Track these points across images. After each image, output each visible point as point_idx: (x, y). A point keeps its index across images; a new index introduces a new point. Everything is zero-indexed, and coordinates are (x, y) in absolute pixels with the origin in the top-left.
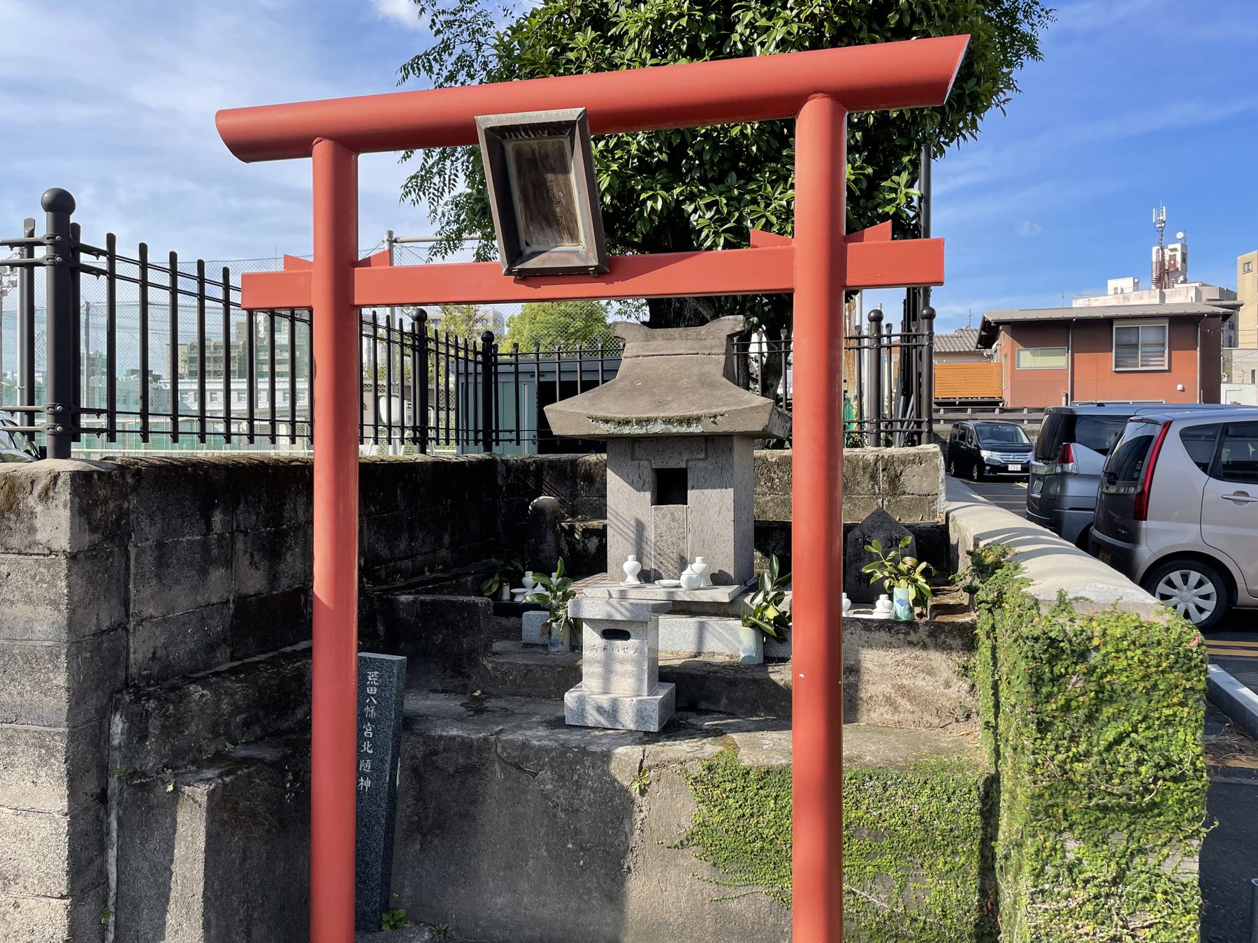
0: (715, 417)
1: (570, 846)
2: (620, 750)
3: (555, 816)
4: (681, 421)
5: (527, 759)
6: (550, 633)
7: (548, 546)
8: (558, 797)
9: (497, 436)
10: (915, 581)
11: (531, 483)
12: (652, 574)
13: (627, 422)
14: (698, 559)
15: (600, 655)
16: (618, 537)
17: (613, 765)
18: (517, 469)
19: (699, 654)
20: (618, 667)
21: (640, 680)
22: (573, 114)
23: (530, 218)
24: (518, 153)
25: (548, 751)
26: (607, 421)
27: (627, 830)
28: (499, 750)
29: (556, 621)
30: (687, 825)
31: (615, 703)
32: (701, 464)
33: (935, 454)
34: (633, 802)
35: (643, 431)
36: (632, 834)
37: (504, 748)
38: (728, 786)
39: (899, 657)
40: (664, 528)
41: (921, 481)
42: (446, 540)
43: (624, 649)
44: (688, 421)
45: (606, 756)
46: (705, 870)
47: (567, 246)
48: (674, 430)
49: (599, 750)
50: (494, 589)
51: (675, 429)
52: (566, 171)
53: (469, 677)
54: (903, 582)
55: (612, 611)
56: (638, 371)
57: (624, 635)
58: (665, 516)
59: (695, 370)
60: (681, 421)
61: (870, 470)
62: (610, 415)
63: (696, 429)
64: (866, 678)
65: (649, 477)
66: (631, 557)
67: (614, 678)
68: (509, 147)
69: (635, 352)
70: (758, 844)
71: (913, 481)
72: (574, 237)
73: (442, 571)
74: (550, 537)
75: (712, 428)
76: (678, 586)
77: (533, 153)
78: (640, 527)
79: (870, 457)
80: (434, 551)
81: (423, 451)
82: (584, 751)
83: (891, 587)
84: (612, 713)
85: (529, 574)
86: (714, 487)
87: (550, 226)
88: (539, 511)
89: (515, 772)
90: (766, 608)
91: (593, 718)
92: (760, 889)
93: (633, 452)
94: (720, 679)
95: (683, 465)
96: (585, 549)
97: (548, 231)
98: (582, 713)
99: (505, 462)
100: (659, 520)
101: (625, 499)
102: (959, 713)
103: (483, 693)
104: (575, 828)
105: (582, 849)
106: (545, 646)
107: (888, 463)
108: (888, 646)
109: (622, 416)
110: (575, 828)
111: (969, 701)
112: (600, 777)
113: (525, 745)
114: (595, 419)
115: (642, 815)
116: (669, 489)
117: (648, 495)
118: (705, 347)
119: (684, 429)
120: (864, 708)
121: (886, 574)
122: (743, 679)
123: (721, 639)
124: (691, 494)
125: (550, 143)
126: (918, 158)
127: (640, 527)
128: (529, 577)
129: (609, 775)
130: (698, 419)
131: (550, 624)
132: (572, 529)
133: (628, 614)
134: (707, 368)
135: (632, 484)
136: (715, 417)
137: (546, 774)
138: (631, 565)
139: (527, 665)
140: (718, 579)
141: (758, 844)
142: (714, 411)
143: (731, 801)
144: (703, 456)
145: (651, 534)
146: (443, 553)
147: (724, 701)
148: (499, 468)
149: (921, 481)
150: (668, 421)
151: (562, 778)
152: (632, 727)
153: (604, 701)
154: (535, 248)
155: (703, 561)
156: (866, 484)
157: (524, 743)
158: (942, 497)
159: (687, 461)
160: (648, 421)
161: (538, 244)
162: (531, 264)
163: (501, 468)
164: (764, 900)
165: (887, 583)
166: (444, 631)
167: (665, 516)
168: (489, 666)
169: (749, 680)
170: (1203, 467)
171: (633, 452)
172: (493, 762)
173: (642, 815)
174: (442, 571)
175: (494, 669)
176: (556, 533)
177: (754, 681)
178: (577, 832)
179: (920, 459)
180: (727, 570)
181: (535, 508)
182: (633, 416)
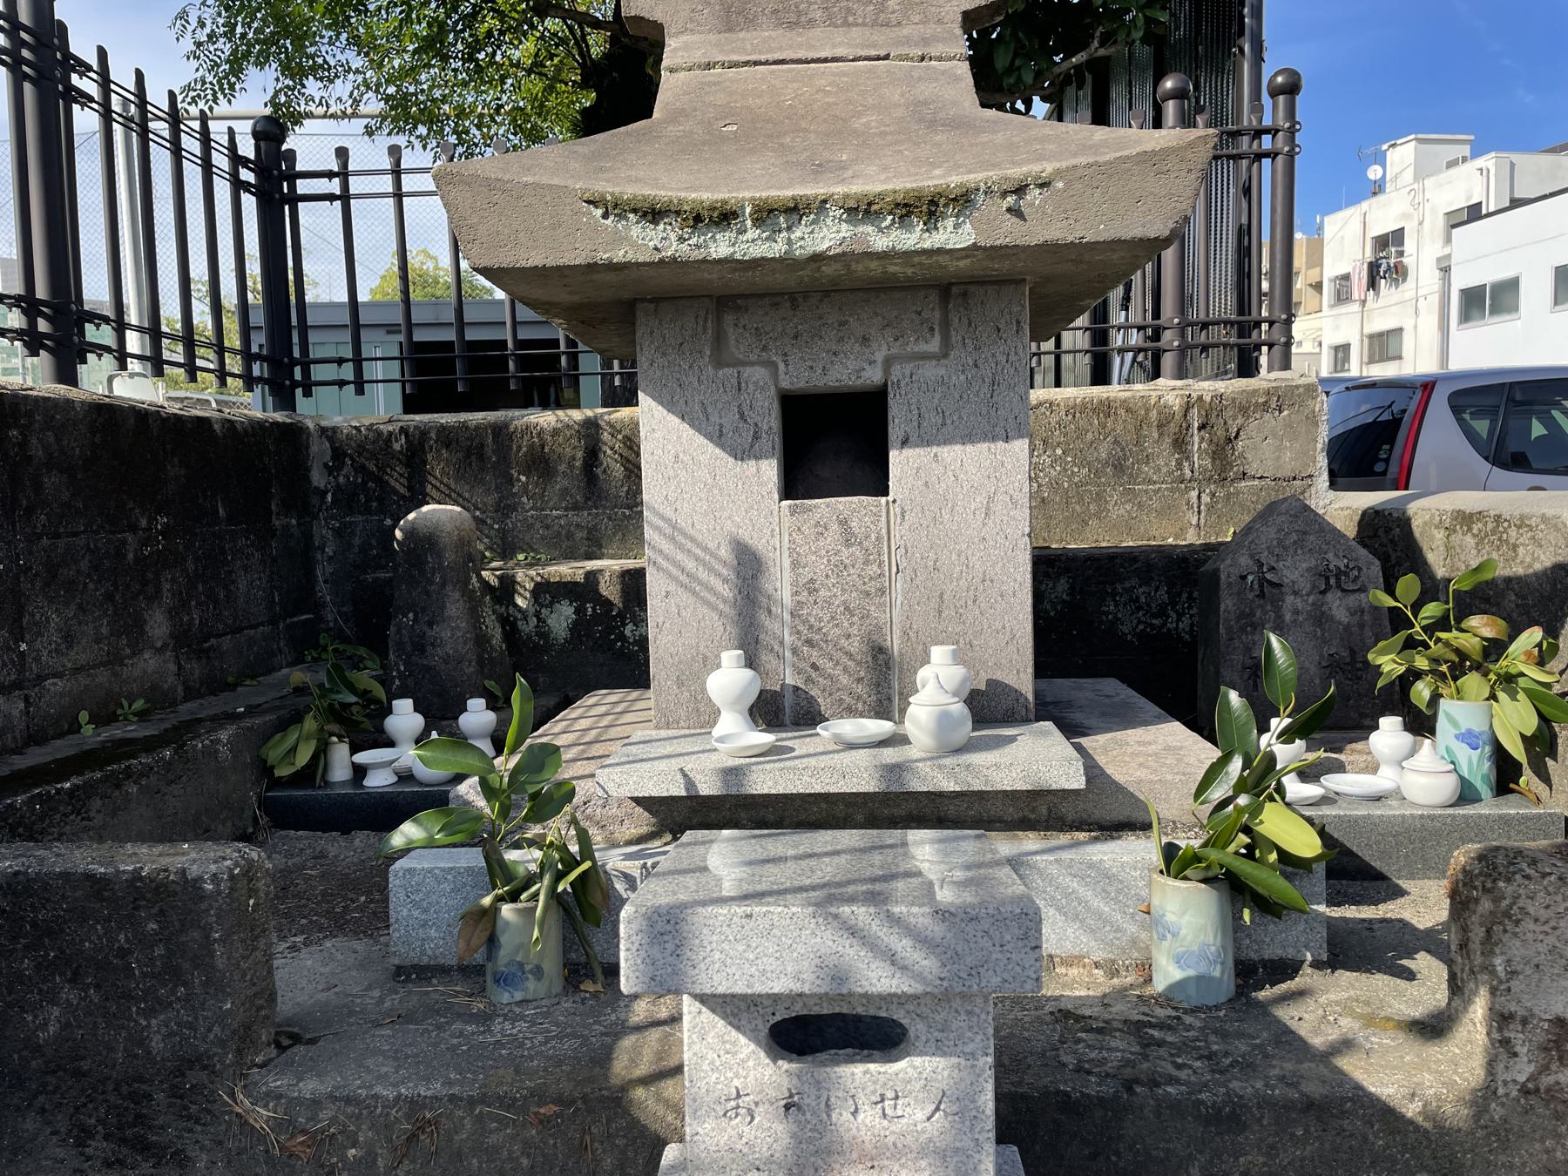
0: (1020, 190)
6: (492, 941)
7: (452, 631)
10: (1509, 680)
11: (397, 481)
12: (788, 701)
13: (725, 217)
14: (939, 653)
16: (685, 597)
18: (361, 448)
26: (653, 214)
29: (513, 897)
32: (930, 371)
35: (776, 249)
40: (822, 566)
41: (1279, 449)
42: (158, 625)
48: (880, 243)
50: (303, 757)
54: (1472, 681)
55: (850, 952)
56: (721, 99)
58: (821, 529)
59: (895, 95)
60: (908, 209)
61: (1173, 428)
63: (954, 235)
65: (771, 420)
66: (731, 657)
69: (699, 56)
73: (143, 716)
74: (455, 607)
75: (1008, 232)
76: (898, 740)
78: (748, 566)
79: (1174, 401)
80: (115, 660)
81: (67, 375)
85: (404, 706)
86: (968, 438)
88: (424, 543)
90: (1256, 810)
94: (1175, 1107)
95: (873, 376)
96: (543, 632)
99: (329, 433)
101: (697, 482)
106: (472, 973)
107: (1211, 415)
109: (706, 196)
114: (616, 208)
116: (832, 445)
117: (770, 470)
118: (907, 41)
119: (913, 238)
121: (1422, 663)
122: (1265, 1103)
124: (900, 461)
128: (405, 717)
130: (963, 200)
131: (493, 911)
132: (508, 586)
134: (925, 90)
135: (718, 437)
136: (1020, 190)
138: (729, 680)
139: (415, 1104)
142: (1016, 172)
144: (934, 345)
145: (781, 585)
146: (149, 663)
148: (314, 449)
149: (1279, 449)
150: (863, 210)
155: (958, 658)
156: (1165, 459)
158: (1323, 480)
159: (888, 363)
160: (795, 210)
163: (319, 450)
165: (1421, 691)
166: (69, 994)
167: (821, 529)
168: (261, 1116)
169: (1289, 1106)
171: (719, 340)
174: (143, 716)
175: (278, 1125)
176: (468, 595)
177: (1310, 1106)
180: (1010, 680)
181: (411, 533)
182: (744, 192)
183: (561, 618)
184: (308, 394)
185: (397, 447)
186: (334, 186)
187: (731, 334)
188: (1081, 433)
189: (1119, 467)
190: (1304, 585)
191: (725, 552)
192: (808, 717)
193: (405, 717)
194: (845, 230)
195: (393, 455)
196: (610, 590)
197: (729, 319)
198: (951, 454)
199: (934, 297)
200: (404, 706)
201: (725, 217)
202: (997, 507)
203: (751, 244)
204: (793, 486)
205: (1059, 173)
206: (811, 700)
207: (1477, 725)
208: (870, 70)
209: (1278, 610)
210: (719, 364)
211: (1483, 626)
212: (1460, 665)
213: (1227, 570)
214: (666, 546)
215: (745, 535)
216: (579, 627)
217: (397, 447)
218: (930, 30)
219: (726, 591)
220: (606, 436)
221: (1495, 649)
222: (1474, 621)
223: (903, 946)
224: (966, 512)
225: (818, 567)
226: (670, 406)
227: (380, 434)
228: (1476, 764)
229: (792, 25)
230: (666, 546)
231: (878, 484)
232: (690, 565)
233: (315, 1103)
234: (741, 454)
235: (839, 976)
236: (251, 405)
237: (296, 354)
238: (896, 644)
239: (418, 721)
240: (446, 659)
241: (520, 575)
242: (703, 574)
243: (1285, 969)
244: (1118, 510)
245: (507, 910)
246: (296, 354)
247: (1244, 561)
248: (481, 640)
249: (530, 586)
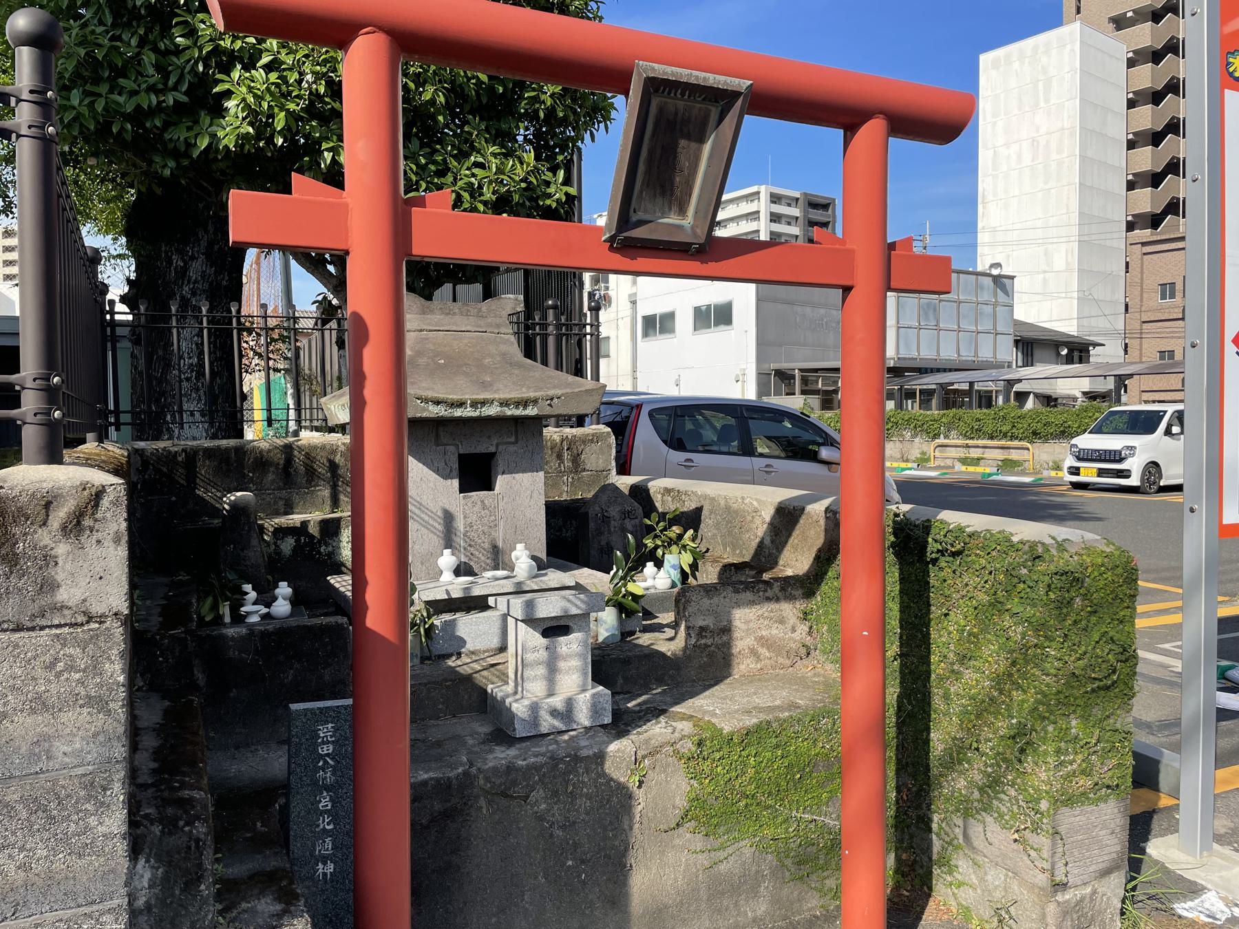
1: (570, 863)
2: (613, 747)
3: (551, 835)
5: (515, 783)
8: (553, 815)
9: (117, 418)
10: (684, 547)
13: (461, 404)
15: (543, 655)
16: (424, 531)
17: (608, 765)
20: (562, 665)
21: (585, 674)
22: (743, 84)
23: (647, 184)
24: (661, 110)
25: (536, 768)
26: (437, 402)
27: (626, 827)
28: (482, 782)
30: (681, 802)
31: (570, 702)
32: (512, 448)
34: (630, 797)
35: (476, 414)
36: (631, 829)
37: (487, 779)
38: (717, 755)
39: (760, 612)
43: (571, 645)
44: (525, 403)
45: (600, 757)
46: (698, 842)
47: (672, 219)
48: (509, 413)
49: (591, 753)
52: (701, 140)
54: (674, 548)
55: (569, 605)
58: (474, 504)
61: (557, 449)
62: (441, 396)
67: (559, 677)
68: (655, 102)
70: (742, 804)
72: (682, 211)
77: (676, 114)
78: (448, 518)
79: (557, 438)
82: (576, 759)
84: (566, 714)
86: (524, 471)
87: (663, 193)
89: (504, 802)
91: (548, 723)
92: (744, 843)
93: (437, 436)
95: (492, 449)
96: (278, 552)
97: (659, 200)
98: (535, 720)
100: (467, 507)
102: (803, 651)
104: (575, 843)
105: (583, 862)
107: (571, 442)
108: (752, 603)
109: (454, 397)
110: (575, 843)
111: (808, 640)
112: (595, 781)
113: (510, 768)
115: (640, 807)
116: (476, 475)
118: (490, 325)
119: (519, 412)
120: (735, 661)
122: (636, 656)
124: (501, 482)
125: (698, 107)
126: (572, 159)
127: (448, 518)
129: (604, 775)
130: (535, 401)
135: (437, 471)
137: (538, 794)
141: (742, 804)
142: (551, 393)
143: (719, 769)
144: (512, 439)
145: (460, 525)
147: (620, 681)
150: (504, 403)
151: (555, 793)
152: (587, 723)
153: (557, 702)
154: (641, 215)
157: (508, 767)
158: (614, 472)
159: (497, 446)
160: (483, 403)
161: (645, 211)
162: (637, 233)
164: (748, 852)
165: (660, 552)
166: (297, 665)
167: (474, 504)
170: (665, 442)
171: (437, 436)
172: (477, 797)
173: (640, 807)
177: (646, 656)
178: (576, 845)
179: (596, 438)
182: (468, 396)
183: (288, 545)
184: (117, 429)
185: (180, 459)
187: (442, 434)
190: (617, 517)
191: (440, 513)
194: (499, 409)
196: (314, 530)
197: (441, 429)
198: (519, 476)
200: (248, 587)
201: (461, 404)
202: (535, 495)
203: (468, 412)
204: (463, 489)
206: (471, 567)
211: (676, 529)
212: (671, 542)
213: (594, 510)
214: (417, 511)
215: (447, 507)
216: (297, 548)
217: (180, 459)
218: (498, 320)
219: (440, 528)
220: (296, 453)
221: (680, 537)
222: (674, 528)
223: (578, 603)
226: (419, 460)
227: (170, 452)
228: (676, 575)
229: (448, 314)
230: (417, 511)
232: (427, 518)
234: (445, 477)
237: (111, 407)
238: (500, 545)
242: (431, 522)
243: (633, 633)
246: (111, 407)
249: (271, 529)
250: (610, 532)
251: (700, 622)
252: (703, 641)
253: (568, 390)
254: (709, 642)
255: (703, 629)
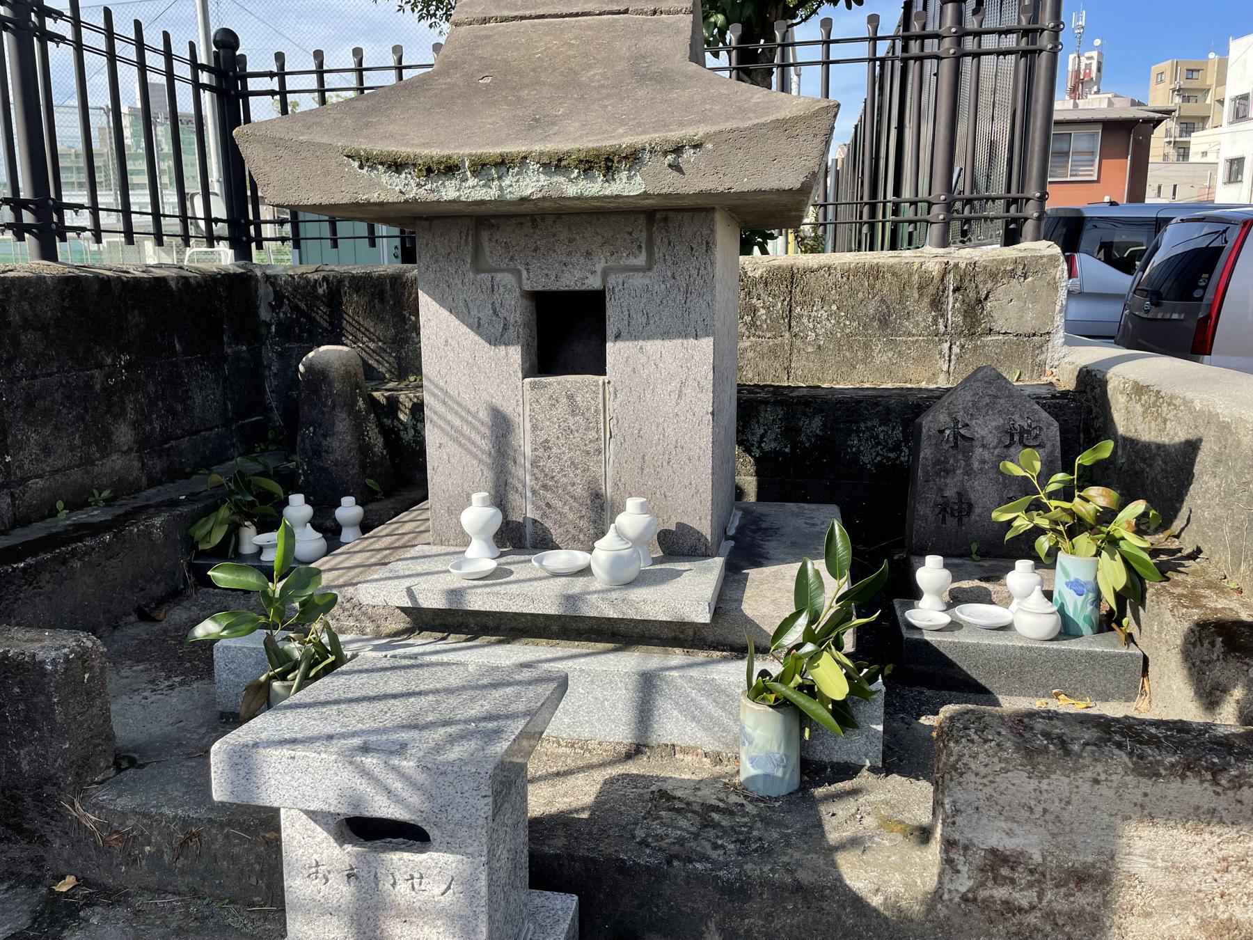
0: (678, 150)
4: (589, 164)
7: (340, 440)
9: (258, 231)
10: (1113, 542)
11: (321, 315)
12: (529, 530)
13: (450, 169)
14: (632, 504)
15: (340, 891)
18: (296, 288)
19: (636, 751)
26: (397, 166)
32: (638, 281)
33: (1052, 258)
35: (491, 193)
39: (1232, 850)
40: (554, 430)
41: (1022, 310)
42: (124, 434)
48: (571, 190)
50: (217, 537)
51: (574, 187)
53: (45, 842)
54: (1083, 540)
55: (362, 786)
56: (486, 51)
57: (411, 835)
58: (554, 402)
59: (623, 48)
60: (589, 164)
61: (931, 290)
64: (1126, 897)
65: (517, 312)
69: (478, 12)
71: (1008, 310)
73: (109, 502)
74: (342, 424)
76: (586, 571)
78: (501, 426)
79: (934, 267)
80: (87, 462)
81: (48, 253)
83: (1053, 552)
85: (297, 499)
86: (666, 335)
88: (318, 376)
90: (814, 657)
93: (477, 252)
94: (701, 879)
95: (594, 283)
99: (271, 280)
101: (463, 366)
103: (83, 881)
107: (965, 278)
108: (1206, 816)
109: (436, 152)
114: (367, 161)
116: (565, 335)
117: (515, 355)
119: (595, 187)
121: (1044, 523)
122: (766, 883)
123: (692, 713)
124: (613, 350)
127: (501, 426)
128: (298, 508)
130: (633, 158)
133: (414, 799)
134: (649, 43)
135: (477, 327)
136: (678, 150)
138: (478, 515)
139: (186, 822)
140: (676, 545)
142: (676, 135)
144: (641, 260)
145: (524, 442)
146: (116, 462)
148: (261, 291)
149: (1022, 310)
150: (555, 164)
155: (644, 509)
156: (923, 315)
158: (1059, 337)
160: (503, 164)
163: (265, 292)
165: (1043, 544)
167: (554, 402)
168: (91, 819)
169: (783, 887)
171: (477, 252)
174: (109, 502)
175: (101, 826)
179: (1023, 269)
180: (695, 524)
182: (463, 150)
184: (260, 247)
185: (320, 291)
186: (274, 84)
187: (486, 244)
188: (853, 292)
189: (884, 321)
190: (992, 440)
191: (484, 415)
192: (544, 543)
193: (298, 508)
195: (318, 297)
197: (485, 235)
199: (642, 220)
200: (297, 499)
201: (450, 169)
202: (688, 391)
205: (708, 136)
206: (546, 531)
207: (1084, 575)
208: (611, 24)
209: (968, 459)
210: (478, 270)
211: (1099, 497)
212: (1076, 527)
214: (441, 409)
215: (498, 402)
217: (320, 291)
219: (485, 444)
221: (1107, 516)
223: (397, 785)
224: (662, 398)
225: (551, 431)
226: (442, 301)
227: (308, 281)
228: (1079, 608)
230: (441, 409)
231: (598, 367)
232: (458, 423)
233: (124, 815)
234: (494, 341)
235: (357, 802)
236: (224, 257)
237: (251, 217)
238: (609, 492)
239: (308, 510)
240: (336, 463)
241: (402, 398)
242: (466, 430)
244: (882, 355)
245: (276, 685)
246: (251, 217)
247: (943, 418)
248: (364, 448)
249: (409, 405)
250: (969, 472)
251: (994, 836)
252: (1001, 893)
253: (729, 125)
254: (1023, 898)
255: (998, 863)
